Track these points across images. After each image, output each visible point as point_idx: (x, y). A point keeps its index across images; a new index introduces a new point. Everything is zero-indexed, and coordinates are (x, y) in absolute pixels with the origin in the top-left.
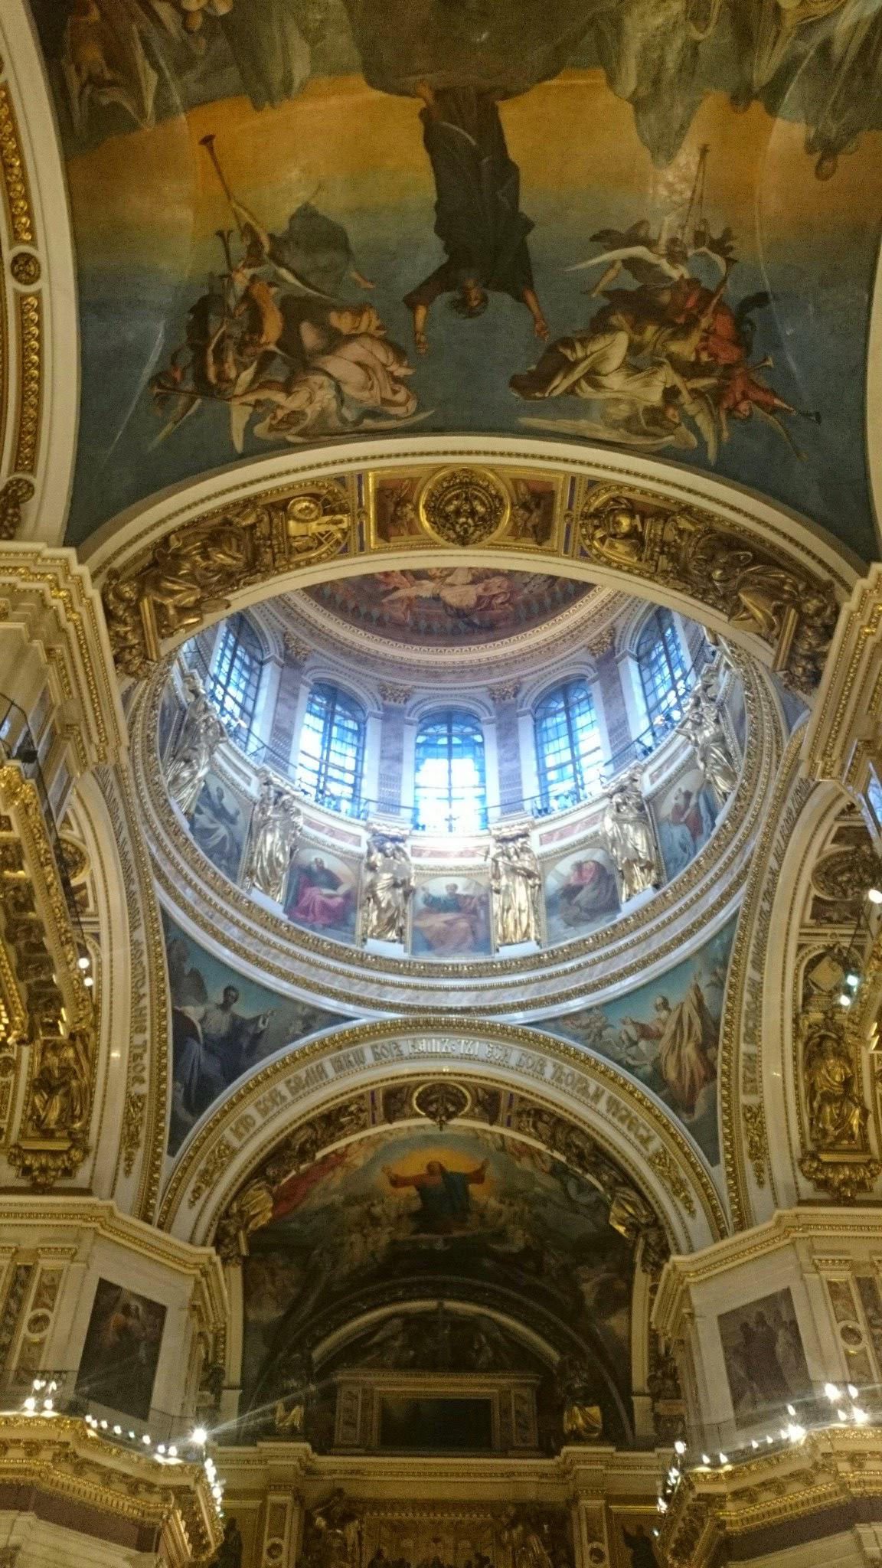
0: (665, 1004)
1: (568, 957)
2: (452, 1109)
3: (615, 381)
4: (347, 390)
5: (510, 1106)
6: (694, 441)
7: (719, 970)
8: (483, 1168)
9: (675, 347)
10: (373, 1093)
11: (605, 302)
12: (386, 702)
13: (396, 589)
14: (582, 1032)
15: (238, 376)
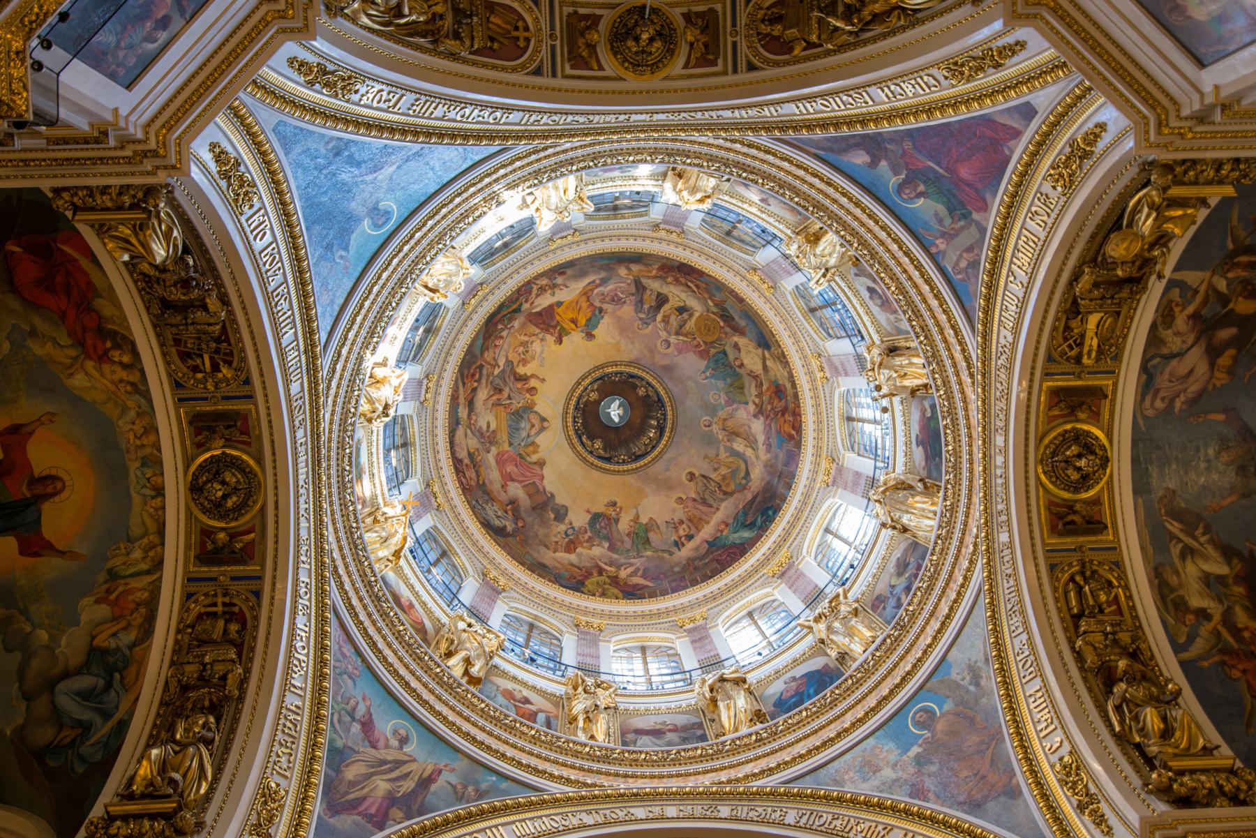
0: (404, 741)
1: (384, 615)
2: (230, 503)
3: (1191, 570)
4: (1175, 362)
5: (233, 579)
6: (1182, 640)
7: (470, 789)
8: (62, 553)
9: (1238, 610)
10: (251, 397)
11: (1246, 554)
12: (425, 381)
13: (464, 384)
14: (337, 647)
15: (1226, 279)
